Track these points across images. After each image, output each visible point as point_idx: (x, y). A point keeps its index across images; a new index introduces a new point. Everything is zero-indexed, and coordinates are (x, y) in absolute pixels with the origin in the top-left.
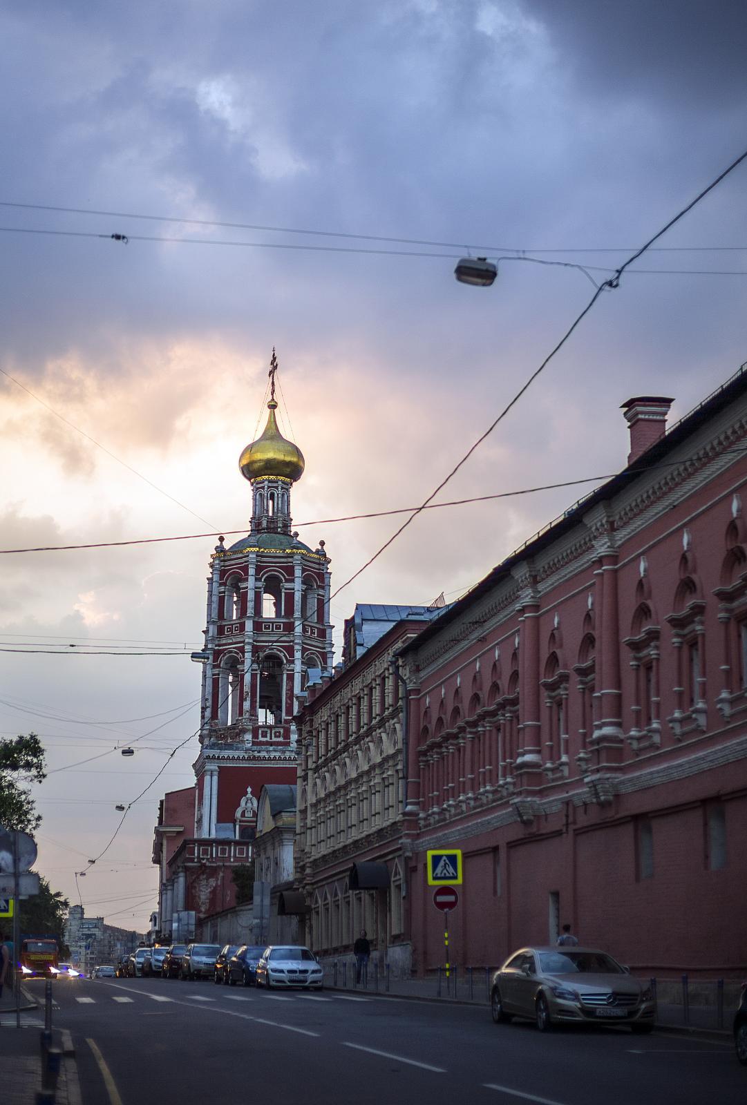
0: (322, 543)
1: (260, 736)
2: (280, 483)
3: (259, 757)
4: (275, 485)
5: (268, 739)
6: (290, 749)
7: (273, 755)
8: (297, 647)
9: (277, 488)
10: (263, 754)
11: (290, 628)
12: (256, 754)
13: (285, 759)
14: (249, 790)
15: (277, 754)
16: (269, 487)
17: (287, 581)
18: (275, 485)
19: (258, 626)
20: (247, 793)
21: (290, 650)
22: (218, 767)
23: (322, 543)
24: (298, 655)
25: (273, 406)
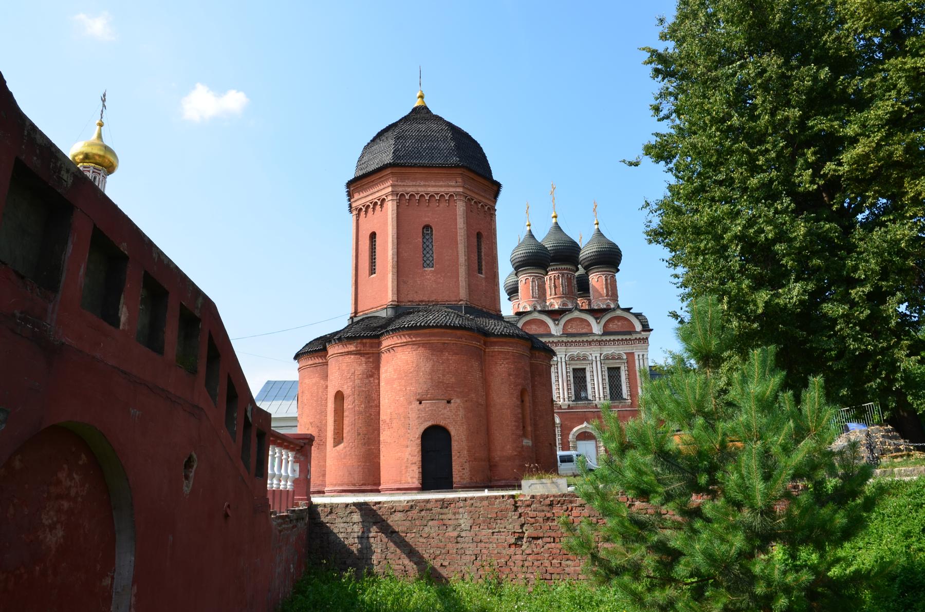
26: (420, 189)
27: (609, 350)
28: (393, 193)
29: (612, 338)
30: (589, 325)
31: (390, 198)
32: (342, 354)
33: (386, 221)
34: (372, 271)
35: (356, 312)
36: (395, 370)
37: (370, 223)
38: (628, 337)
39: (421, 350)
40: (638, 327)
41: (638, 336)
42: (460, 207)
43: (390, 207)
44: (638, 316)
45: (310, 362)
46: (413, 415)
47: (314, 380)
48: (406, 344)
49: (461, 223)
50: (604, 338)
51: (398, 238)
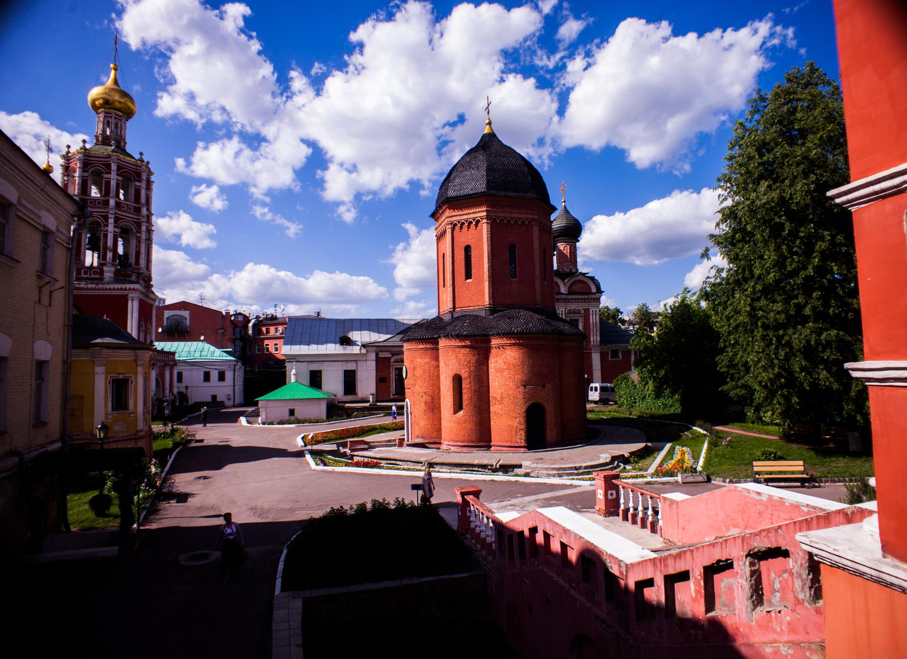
0: (141, 154)
7: (90, 286)
11: (107, 203)
15: (93, 286)
17: (107, 173)
21: (106, 218)
23: (141, 154)
24: (111, 221)
26: (508, 215)
27: (572, 306)
28: (488, 217)
29: (574, 297)
30: (558, 286)
31: (485, 221)
32: (459, 347)
33: (481, 239)
34: (468, 275)
35: (454, 307)
36: (505, 363)
37: (465, 237)
38: (586, 297)
39: (524, 350)
40: (594, 290)
41: (594, 296)
42: (536, 231)
43: (485, 227)
44: (592, 279)
45: (421, 346)
46: (520, 396)
47: (426, 360)
48: (514, 344)
49: (536, 244)
50: (569, 297)
51: (492, 254)
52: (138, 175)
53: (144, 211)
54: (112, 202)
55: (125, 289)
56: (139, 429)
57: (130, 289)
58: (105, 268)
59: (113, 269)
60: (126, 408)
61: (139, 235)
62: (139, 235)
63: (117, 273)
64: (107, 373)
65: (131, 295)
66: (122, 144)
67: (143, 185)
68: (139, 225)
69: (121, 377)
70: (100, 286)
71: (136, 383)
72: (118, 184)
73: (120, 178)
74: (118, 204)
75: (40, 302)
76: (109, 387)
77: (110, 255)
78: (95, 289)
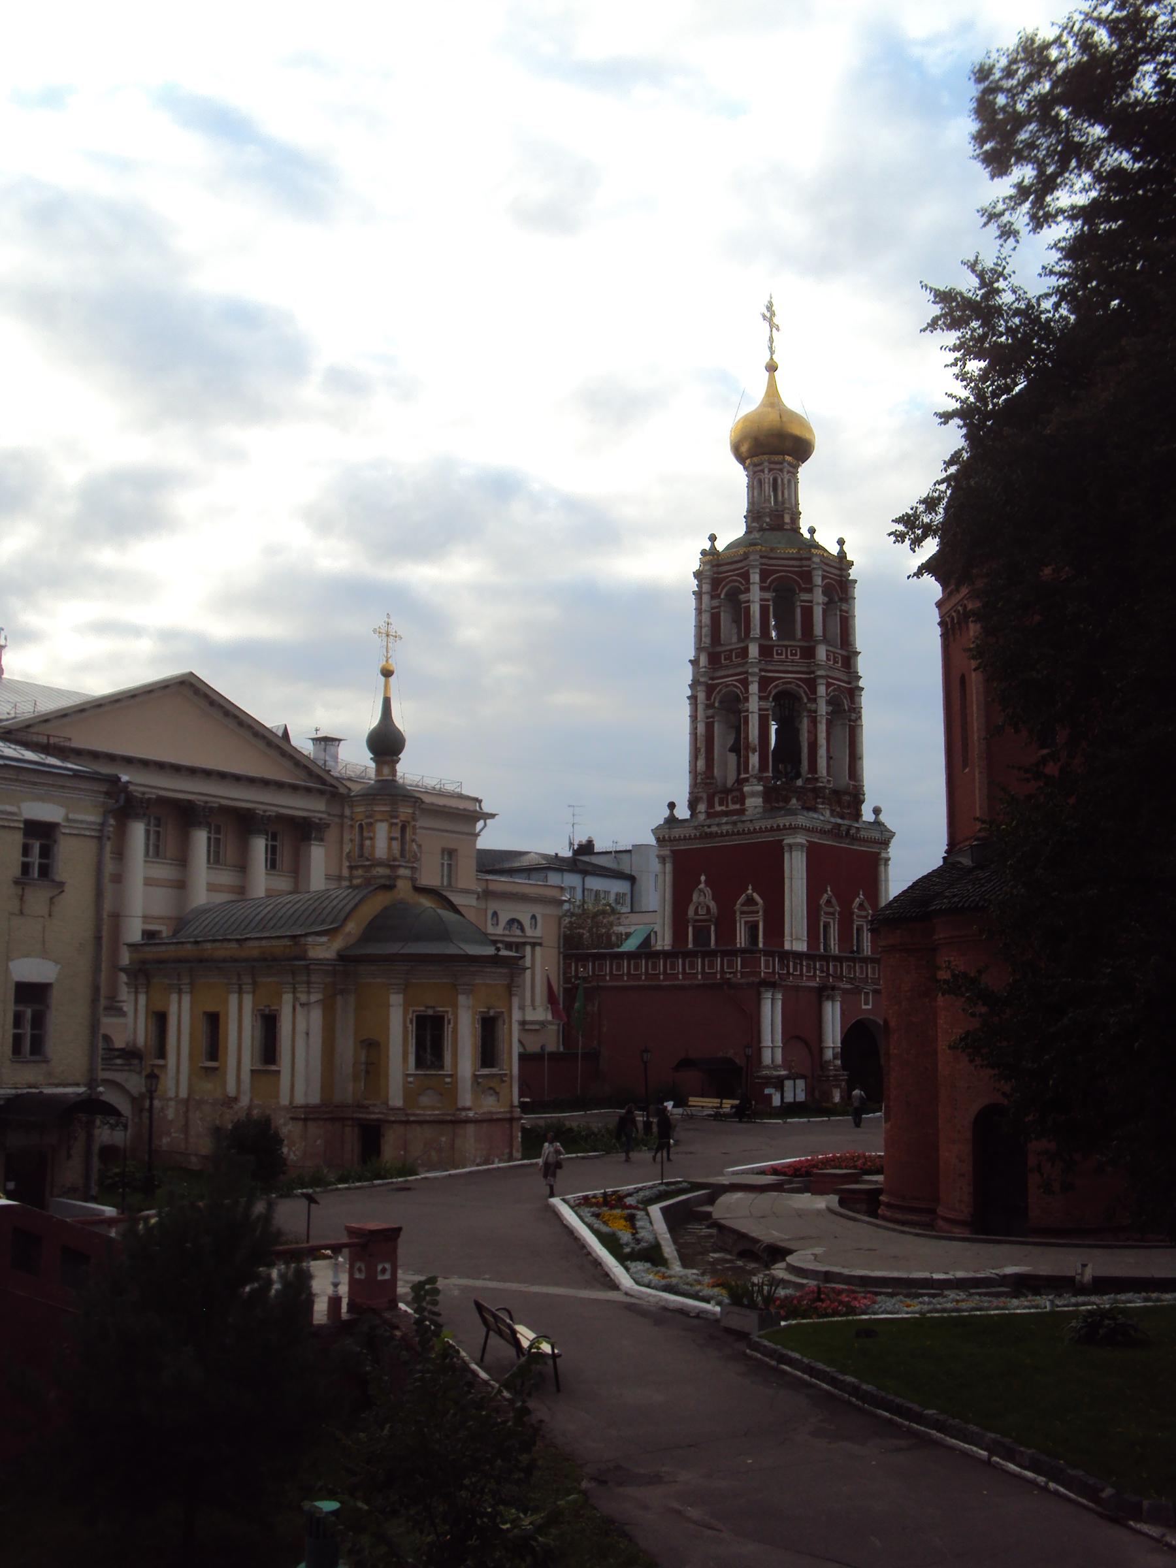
1: (717, 804)
2: (766, 464)
3: (711, 833)
4: (759, 468)
5: (724, 808)
6: (745, 818)
7: (725, 828)
8: (750, 679)
9: (762, 471)
10: (714, 829)
12: (708, 830)
13: (738, 833)
14: (703, 878)
15: (729, 827)
16: (755, 473)
18: (759, 468)
19: (714, 659)
20: (700, 882)
21: (745, 683)
22: (673, 852)
24: (754, 688)
25: (772, 368)
52: (807, 576)
53: (821, 652)
54: (754, 650)
55: (778, 829)
56: (460, 1104)
57: (785, 828)
58: (746, 789)
59: (760, 788)
60: (442, 1067)
61: (813, 706)
62: (813, 706)
63: (769, 795)
64: (407, 1005)
65: (788, 840)
66: (787, 519)
67: (819, 597)
68: (812, 684)
69: (430, 1012)
70: (740, 826)
71: (456, 1023)
72: (764, 610)
73: (768, 595)
74: (766, 651)
75: (22, 913)
76: (412, 1028)
77: (754, 759)
78: (733, 834)
